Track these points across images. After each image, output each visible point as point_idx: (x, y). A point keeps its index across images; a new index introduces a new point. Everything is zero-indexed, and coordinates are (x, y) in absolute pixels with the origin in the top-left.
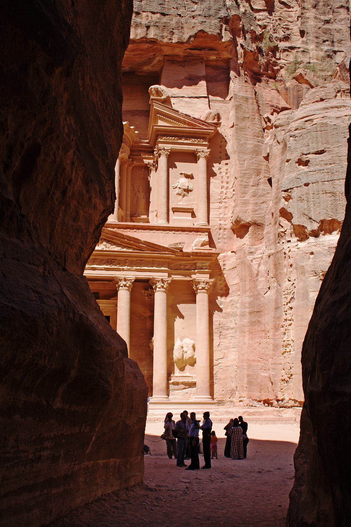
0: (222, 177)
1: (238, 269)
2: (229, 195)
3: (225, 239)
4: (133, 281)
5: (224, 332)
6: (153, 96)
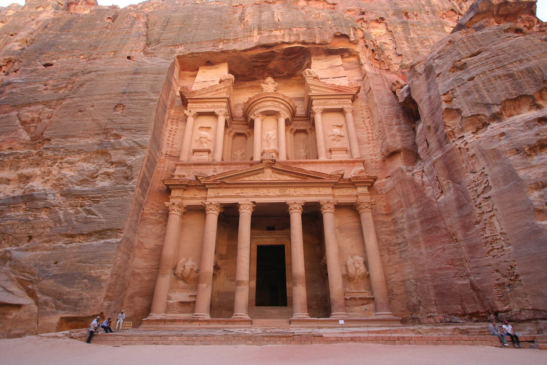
0: (367, 127)
1: (397, 188)
2: (375, 138)
3: (378, 169)
4: (303, 204)
5: (392, 248)
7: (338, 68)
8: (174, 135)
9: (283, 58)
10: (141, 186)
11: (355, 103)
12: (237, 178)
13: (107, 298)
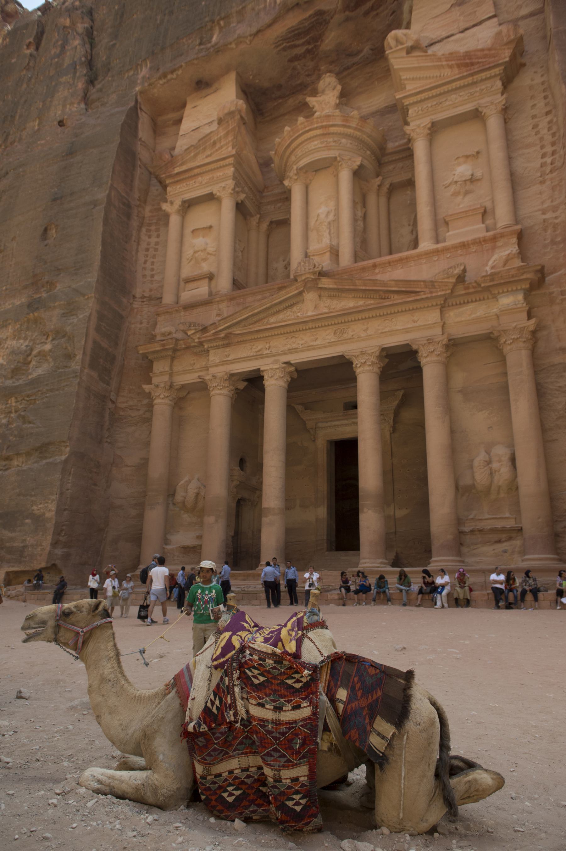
0: (542, 139)
2: (558, 164)
4: (377, 354)
6: (391, 48)
8: (154, 257)
9: (348, 19)
10: (93, 365)
11: (516, 83)
12: (256, 322)
13: (55, 544)
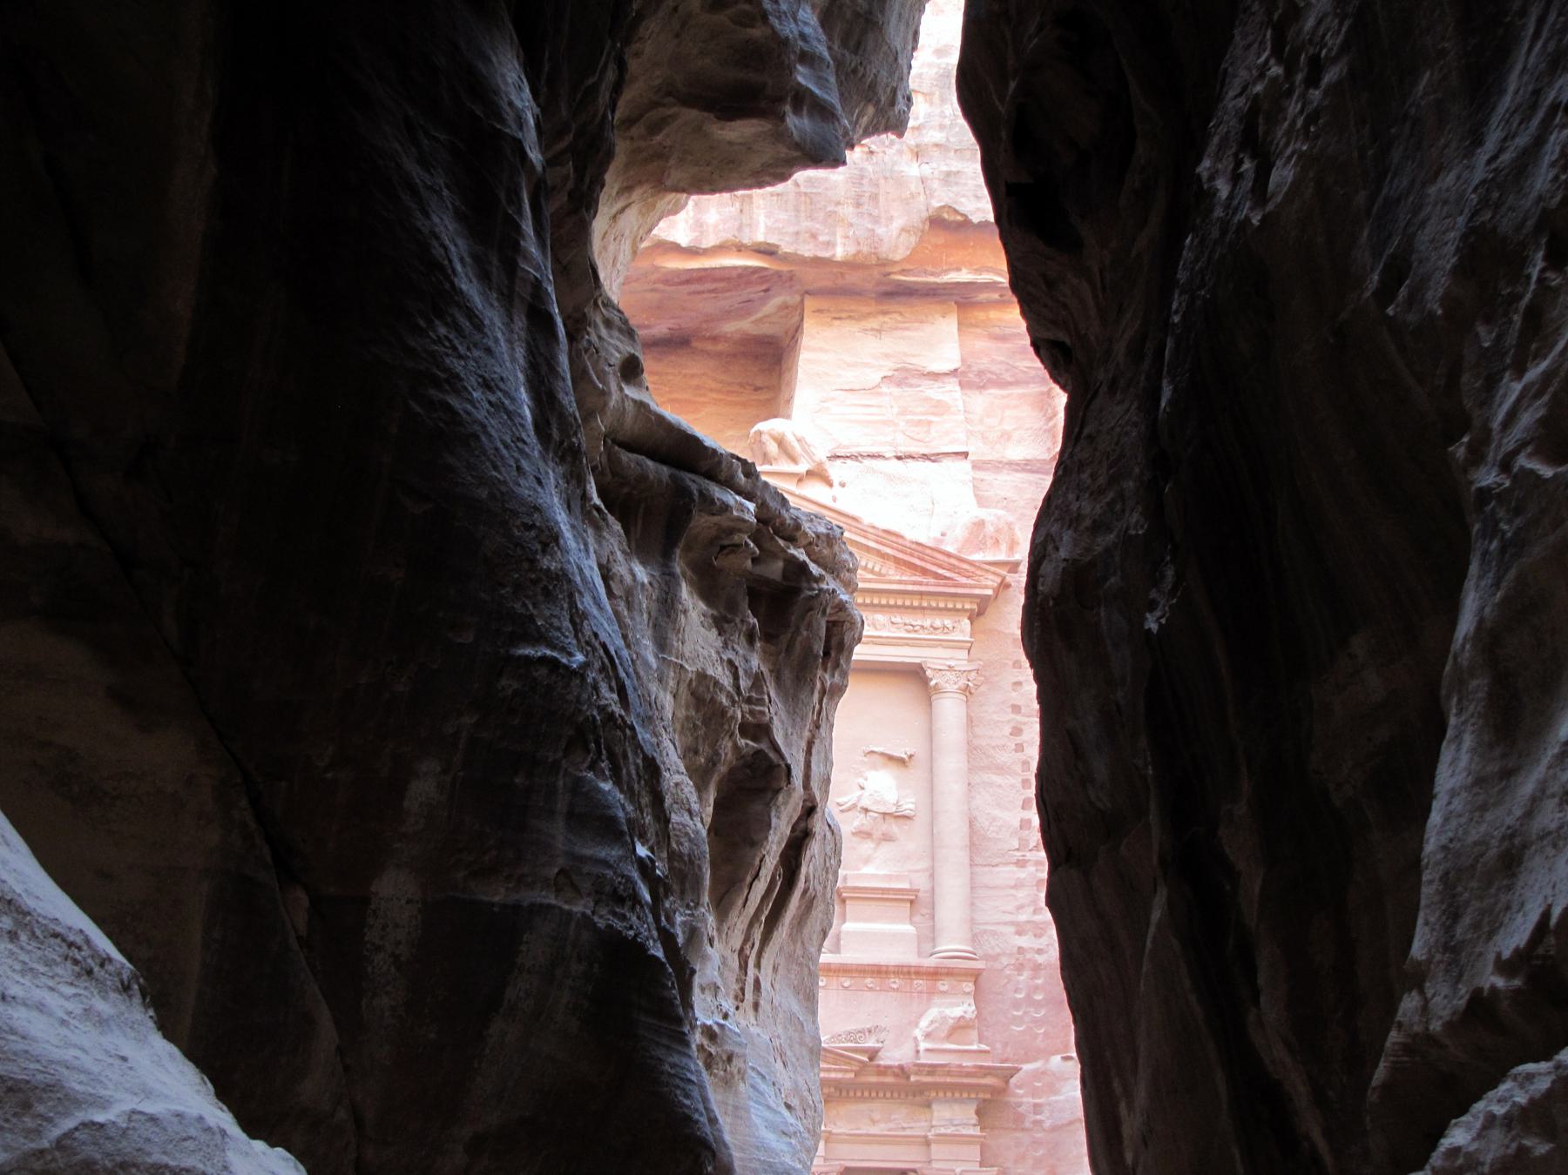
3: (1038, 1005)
7: (934, 391)
11: (987, 621)
